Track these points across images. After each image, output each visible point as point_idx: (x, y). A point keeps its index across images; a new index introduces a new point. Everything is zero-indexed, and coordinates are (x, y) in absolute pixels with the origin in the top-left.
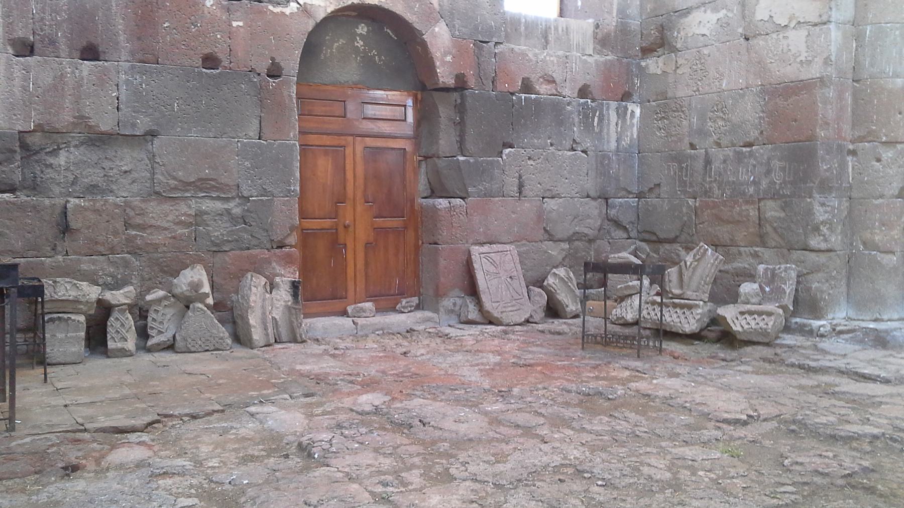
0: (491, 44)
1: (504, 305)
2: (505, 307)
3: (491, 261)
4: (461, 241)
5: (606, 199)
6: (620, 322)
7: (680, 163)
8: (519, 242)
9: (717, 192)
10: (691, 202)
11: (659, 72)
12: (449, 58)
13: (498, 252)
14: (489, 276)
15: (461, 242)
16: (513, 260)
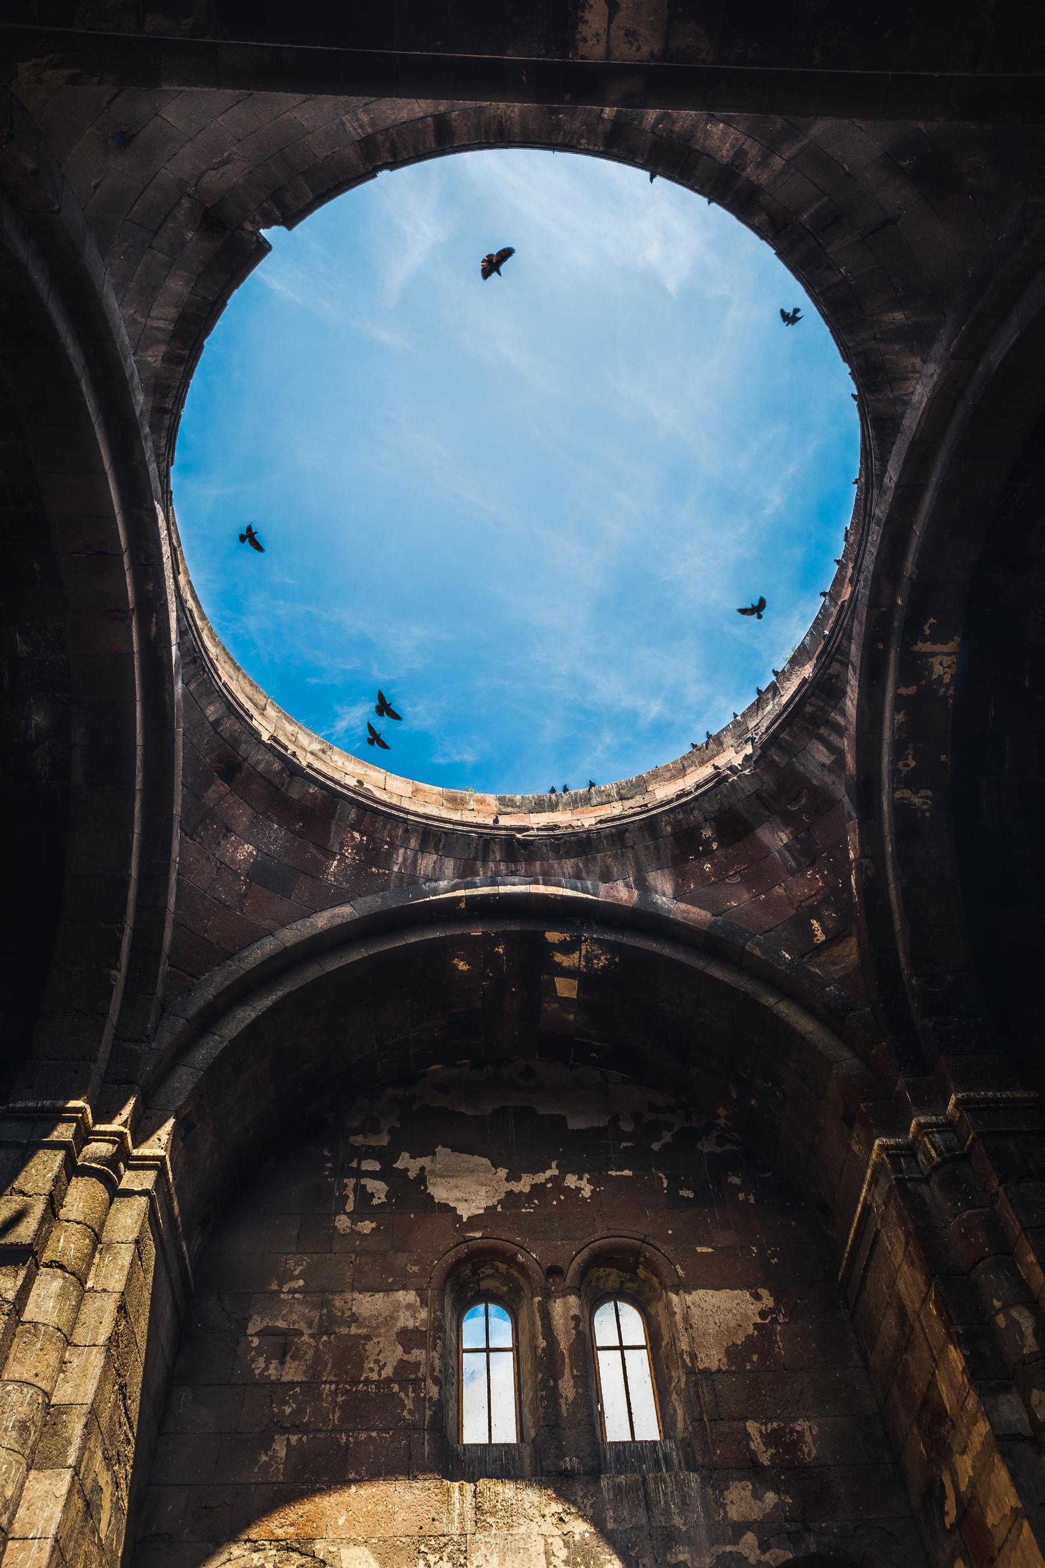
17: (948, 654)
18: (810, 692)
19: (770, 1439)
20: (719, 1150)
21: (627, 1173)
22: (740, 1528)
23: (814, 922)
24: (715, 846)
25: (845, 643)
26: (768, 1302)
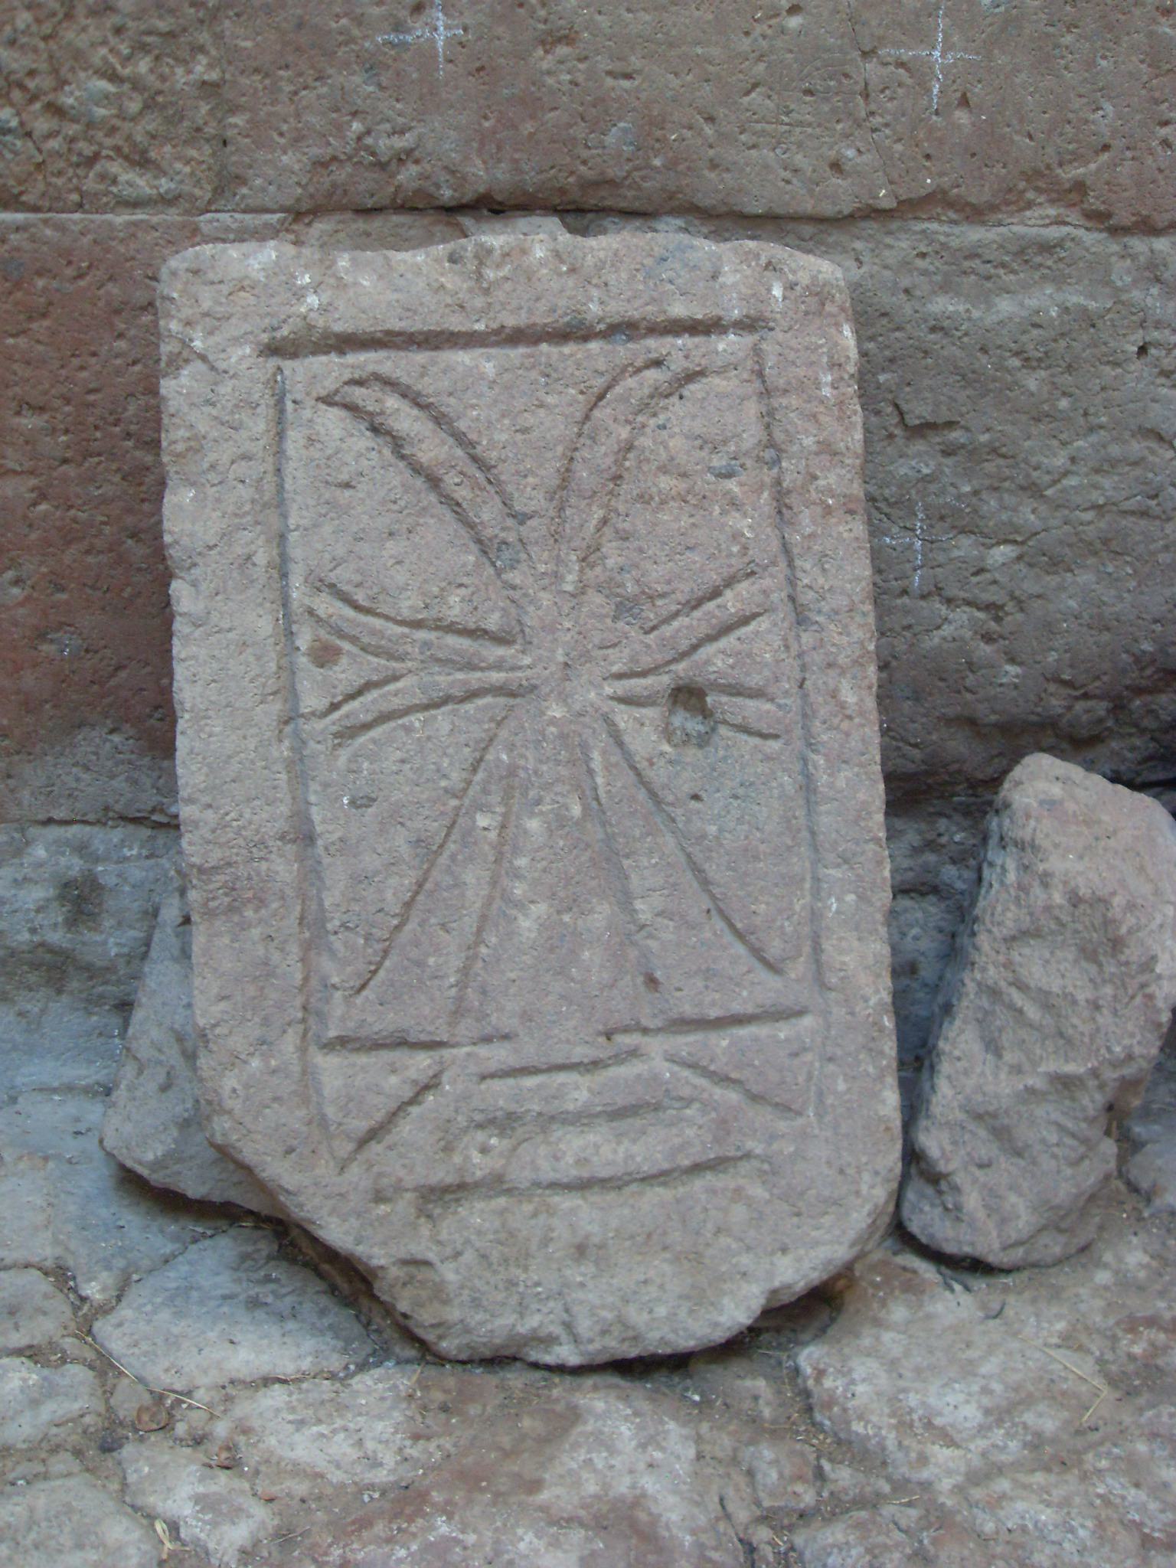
1: (500, 1094)
2: (505, 1123)
3: (432, 448)
4: (141, 161)
8: (976, 214)
13: (574, 332)
14: (345, 673)
15: (140, 183)
16: (773, 449)
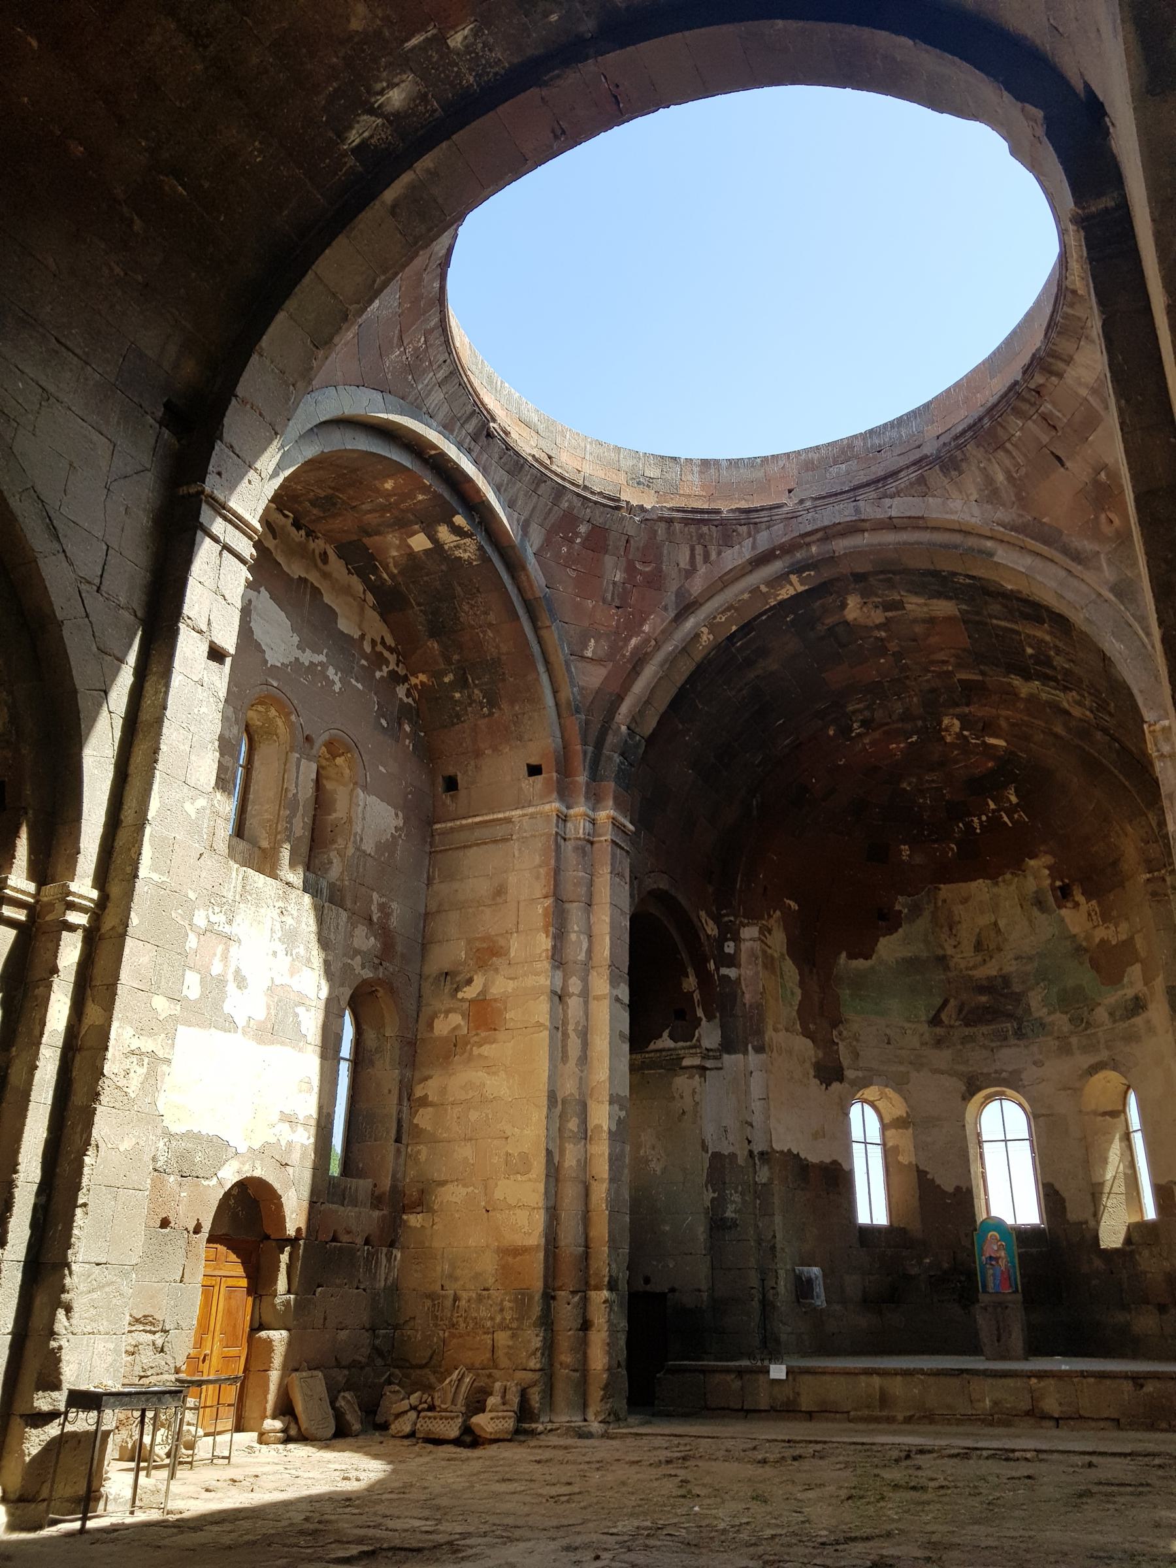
0: (319, 1204)
5: (374, 1331)
6: (400, 1435)
7: (433, 1300)
9: (463, 1325)
10: (441, 1333)
11: (419, 1226)
12: (294, 1216)
17: (795, 590)
18: (715, 523)
19: (382, 907)
20: (405, 700)
21: (359, 686)
22: (357, 952)
23: (593, 641)
24: (578, 540)
25: (763, 526)
26: (401, 823)
